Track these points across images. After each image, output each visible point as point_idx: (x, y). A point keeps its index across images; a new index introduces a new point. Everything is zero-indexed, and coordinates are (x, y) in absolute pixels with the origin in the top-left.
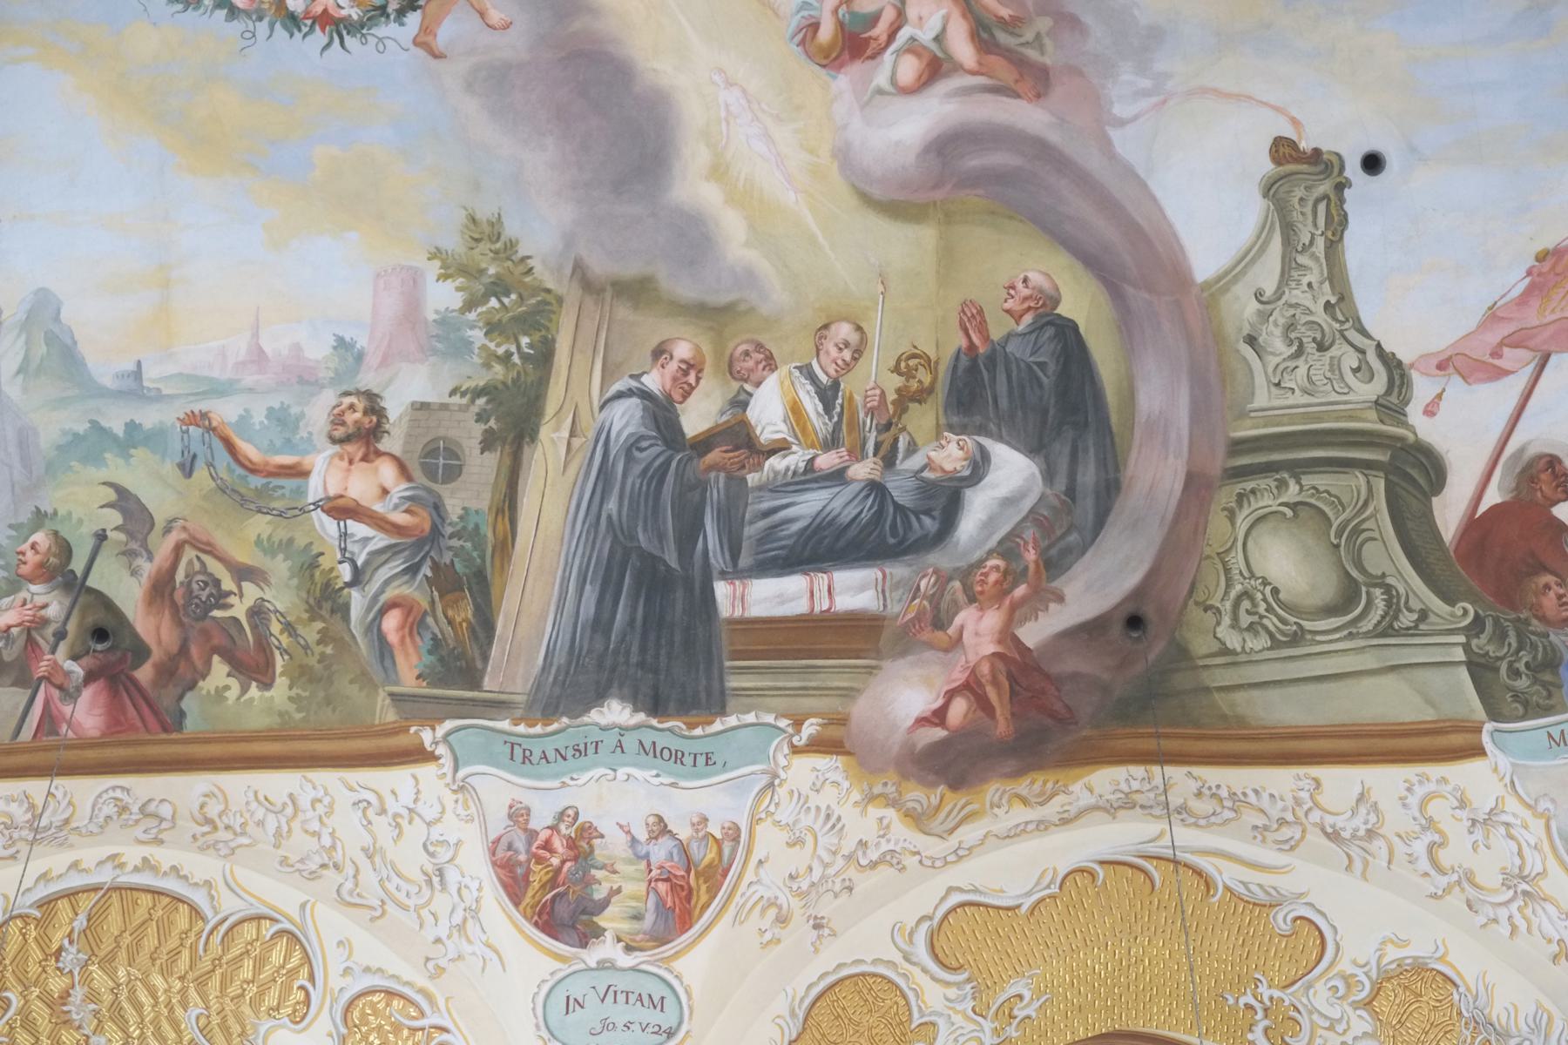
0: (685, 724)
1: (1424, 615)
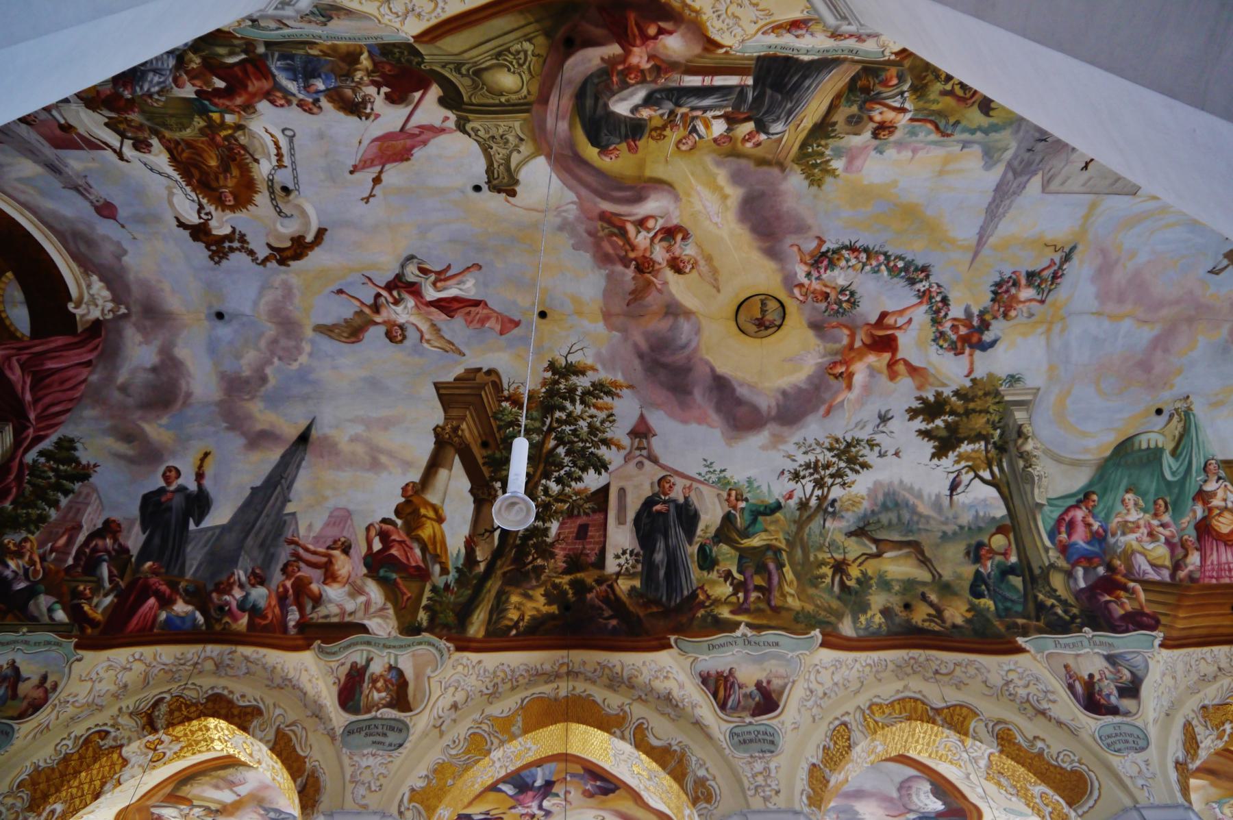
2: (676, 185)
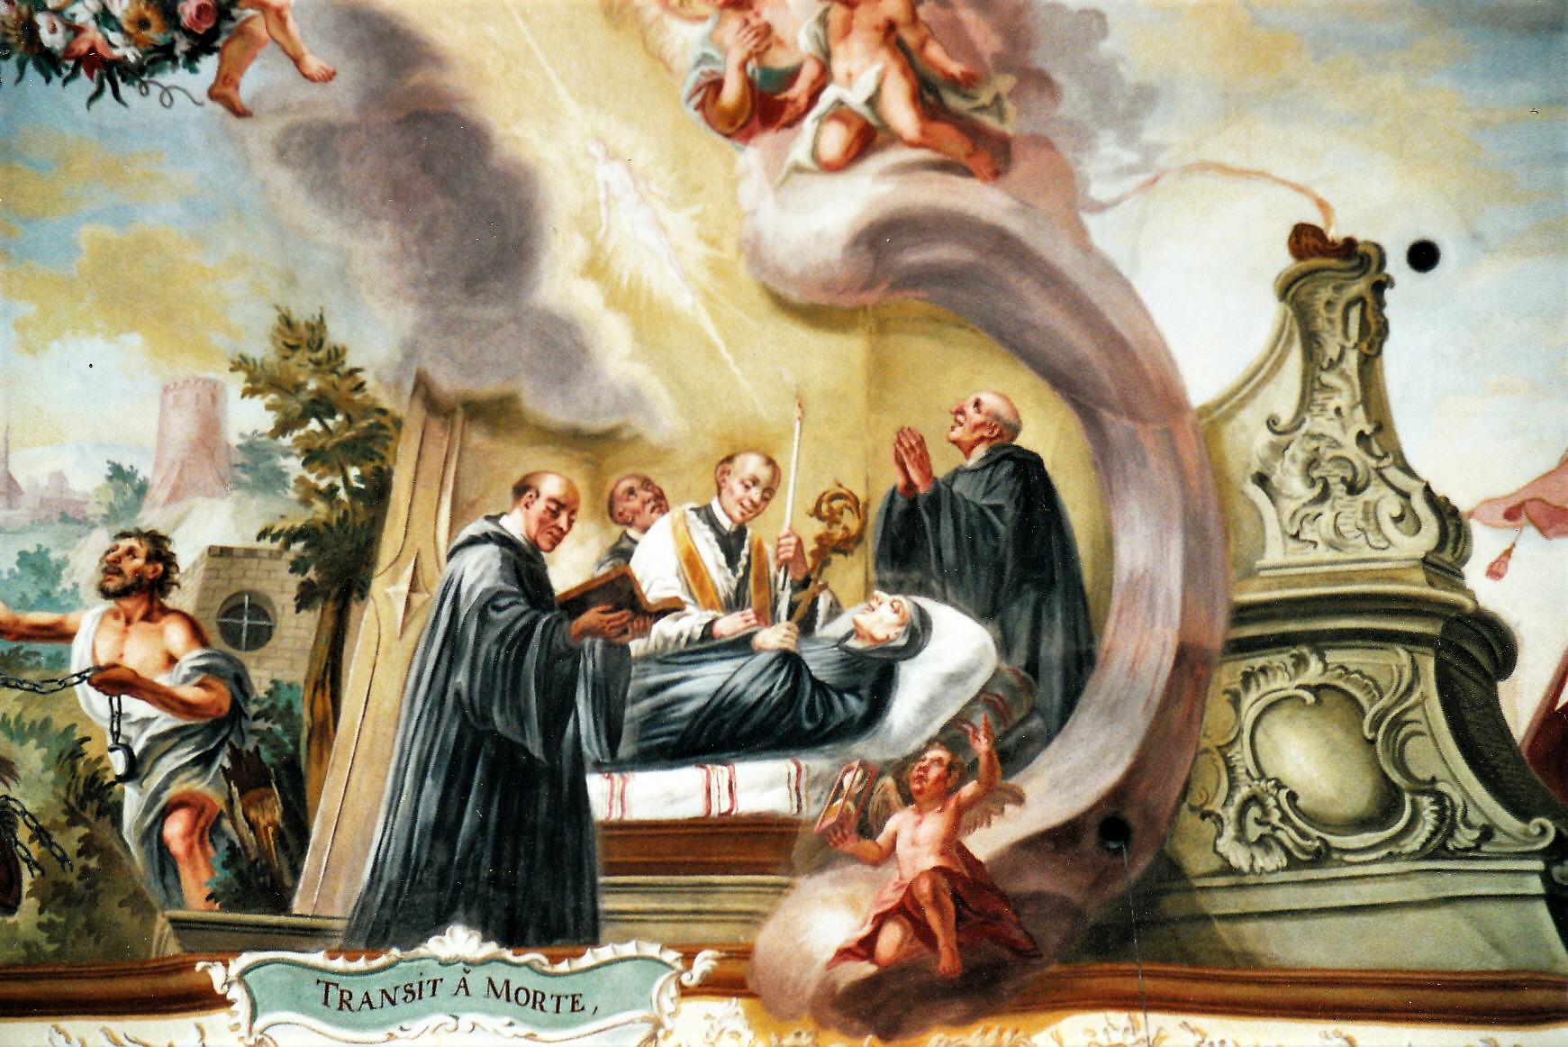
0: (547, 956)
1: (1487, 833)
2: (764, 305)
